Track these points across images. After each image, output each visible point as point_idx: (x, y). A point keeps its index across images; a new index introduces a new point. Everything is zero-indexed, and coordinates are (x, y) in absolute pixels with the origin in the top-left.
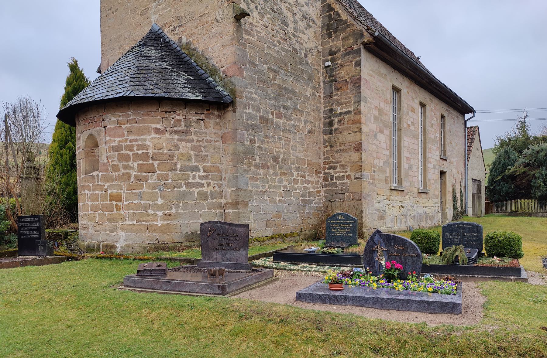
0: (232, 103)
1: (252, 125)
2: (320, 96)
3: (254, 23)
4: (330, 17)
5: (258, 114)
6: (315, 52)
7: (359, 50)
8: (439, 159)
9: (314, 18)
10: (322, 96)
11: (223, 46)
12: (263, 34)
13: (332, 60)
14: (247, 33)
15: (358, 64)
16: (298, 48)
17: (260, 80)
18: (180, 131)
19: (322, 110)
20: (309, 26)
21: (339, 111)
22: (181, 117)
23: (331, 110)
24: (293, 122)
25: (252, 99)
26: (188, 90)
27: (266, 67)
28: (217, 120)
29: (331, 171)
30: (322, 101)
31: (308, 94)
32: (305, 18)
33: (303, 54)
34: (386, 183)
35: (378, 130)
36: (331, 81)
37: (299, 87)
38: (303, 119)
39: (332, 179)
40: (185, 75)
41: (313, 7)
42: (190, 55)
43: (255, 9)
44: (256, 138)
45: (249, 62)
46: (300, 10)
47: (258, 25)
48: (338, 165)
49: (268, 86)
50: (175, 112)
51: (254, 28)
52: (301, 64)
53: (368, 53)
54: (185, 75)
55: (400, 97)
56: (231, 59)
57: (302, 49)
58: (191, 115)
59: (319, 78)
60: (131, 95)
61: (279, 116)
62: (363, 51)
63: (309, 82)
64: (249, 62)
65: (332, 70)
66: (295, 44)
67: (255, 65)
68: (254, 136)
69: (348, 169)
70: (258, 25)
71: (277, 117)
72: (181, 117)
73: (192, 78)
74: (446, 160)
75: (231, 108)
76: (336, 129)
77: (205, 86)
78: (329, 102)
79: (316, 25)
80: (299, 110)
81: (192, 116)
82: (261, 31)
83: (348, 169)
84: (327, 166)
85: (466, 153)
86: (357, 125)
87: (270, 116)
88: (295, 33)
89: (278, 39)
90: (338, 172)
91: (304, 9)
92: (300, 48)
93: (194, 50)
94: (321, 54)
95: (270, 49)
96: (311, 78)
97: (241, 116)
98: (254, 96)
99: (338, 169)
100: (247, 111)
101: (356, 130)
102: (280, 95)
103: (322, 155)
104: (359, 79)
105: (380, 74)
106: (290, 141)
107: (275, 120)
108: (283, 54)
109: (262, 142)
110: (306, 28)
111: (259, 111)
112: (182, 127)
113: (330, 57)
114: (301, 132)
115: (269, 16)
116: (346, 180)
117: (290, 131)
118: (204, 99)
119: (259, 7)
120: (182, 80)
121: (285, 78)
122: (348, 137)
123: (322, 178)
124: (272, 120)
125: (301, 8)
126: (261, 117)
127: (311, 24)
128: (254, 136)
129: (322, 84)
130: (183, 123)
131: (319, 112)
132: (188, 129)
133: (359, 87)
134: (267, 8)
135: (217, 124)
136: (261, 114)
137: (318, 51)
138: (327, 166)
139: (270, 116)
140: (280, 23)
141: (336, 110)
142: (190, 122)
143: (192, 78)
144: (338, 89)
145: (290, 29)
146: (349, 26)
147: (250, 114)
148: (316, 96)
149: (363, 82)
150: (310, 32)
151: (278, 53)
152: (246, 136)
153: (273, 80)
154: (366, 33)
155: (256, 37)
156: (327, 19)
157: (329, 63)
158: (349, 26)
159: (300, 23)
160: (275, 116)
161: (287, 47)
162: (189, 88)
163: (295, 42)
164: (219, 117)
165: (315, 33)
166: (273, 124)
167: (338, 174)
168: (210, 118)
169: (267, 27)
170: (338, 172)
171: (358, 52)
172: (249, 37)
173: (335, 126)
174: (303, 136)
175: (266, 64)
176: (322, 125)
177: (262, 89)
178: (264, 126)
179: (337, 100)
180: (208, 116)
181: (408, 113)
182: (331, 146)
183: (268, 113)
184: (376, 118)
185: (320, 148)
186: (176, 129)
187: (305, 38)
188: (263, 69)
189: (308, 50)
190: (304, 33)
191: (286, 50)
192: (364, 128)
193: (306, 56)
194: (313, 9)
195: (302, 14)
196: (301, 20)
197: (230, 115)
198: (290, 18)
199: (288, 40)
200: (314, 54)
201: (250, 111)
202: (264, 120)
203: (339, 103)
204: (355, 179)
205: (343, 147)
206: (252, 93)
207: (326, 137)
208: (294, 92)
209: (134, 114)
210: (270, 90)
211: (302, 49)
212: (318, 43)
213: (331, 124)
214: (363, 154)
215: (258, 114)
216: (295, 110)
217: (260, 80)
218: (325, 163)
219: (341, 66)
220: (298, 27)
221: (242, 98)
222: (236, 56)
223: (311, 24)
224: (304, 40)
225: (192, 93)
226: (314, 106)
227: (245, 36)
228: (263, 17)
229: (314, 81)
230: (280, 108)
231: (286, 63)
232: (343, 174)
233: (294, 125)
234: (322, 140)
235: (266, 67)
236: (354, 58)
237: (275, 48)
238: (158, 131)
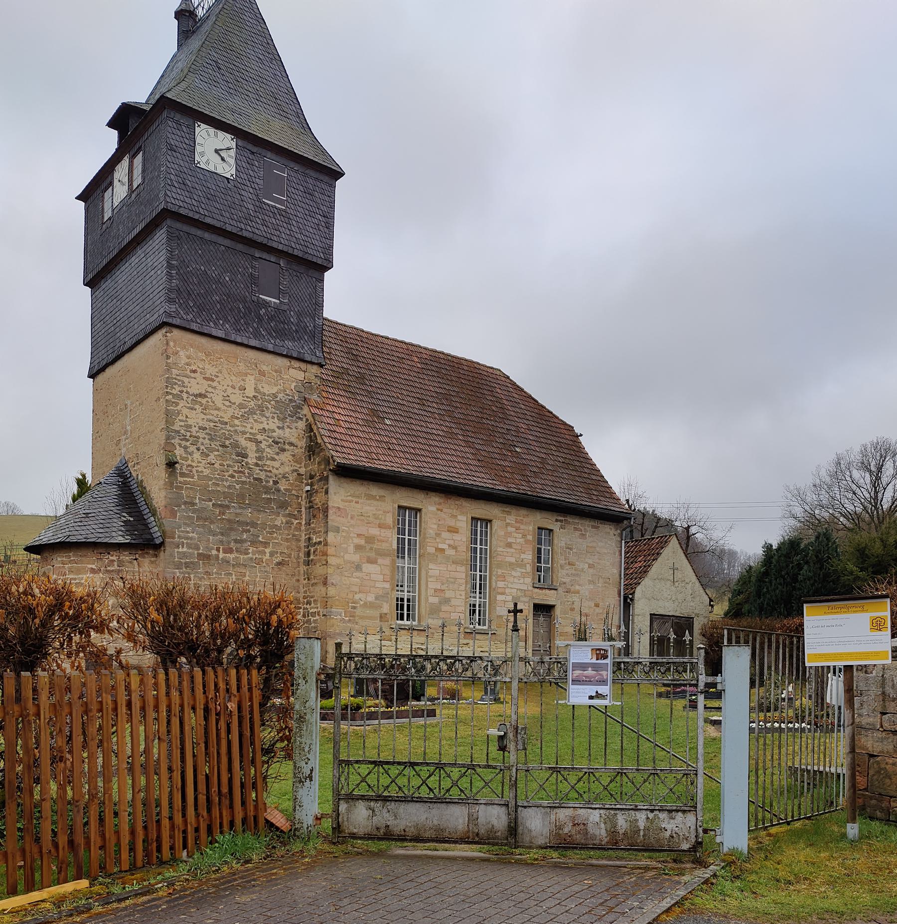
0: (162, 544)
1: (186, 563)
2: (300, 523)
3: (194, 464)
4: (310, 437)
5: (196, 552)
6: (292, 477)
7: (328, 476)
8: (532, 588)
9: (293, 440)
10: (304, 523)
11: (160, 489)
12: (207, 472)
13: (312, 485)
14: (183, 475)
15: (327, 492)
16: (263, 477)
17: (199, 518)
18: (113, 571)
19: (303, 538)
20: (283, 450)
21: (314, 541)
22: (114, 558)
23: (309, 539)
24: (250, 555)
25: (187, 538)
26: (120, 533)
27: (211, 503)
28: (152, 559)
29: (308, 606)
30: (303, 528)
31: (278, 523)
32: (277, 443)
33: (271, 482)
34: (381, 621)
35: (365, 561)
36: (310, 507)
37: (261, 518)
38: (267, 551)
39: (308, 616)
40: (125, 517)
41: (291, 428)
42: (142, 493)
43: (195, 451)
44: (192, 576)
45: (185, 503)
46: (268, 437)
47: (199, 465)
48: (312, 600)
49: (212, 522)
50: (109, 553)
51: (194, 470)
52: (266, 493)
53: (343, 480)
54: (125, 517)
55: (421, 517)
56: (164, 503)
57: (271, 477)
58: (124, 555)
59: (300, 504)
60: (67, 540)
61: (230, 551)
62: (331, 478)
63: (279, 510)
64: (185, 503)
65: (311, 495)
66: (257, 474)
67: (194, 504)
68: (189, 574)
69: (319, 605)
70: (199, 465)
71: (224, 552)
72: (114, 558)
73: (132, 519)
74: (556, 589)
75: (162, 549)
76: (312, 560)
77: (143, 527)
78: (308, 530)
79: (297, 446)
80: (262, 542)
81: (126, 557)
82: (204, 470)
83: (319, 605)
84: (305, 600)
85: (622, 576)
86: (325, 557)
87: (214, 552)
88: (259, 462)
89: (230, 473)
90: (313, 608)
91: (274, 434)
92: (267, 476)
93: (145, 488)
94: (304, 477)
95: (218, 485)
96: (283, 505)
97: (172, 555)
98: (191, 535)
99: (312, 605)
100: (180, 550)
101: (324, 563)
102: (231, 529)
103: (301, 587)
104: (327, 508)
105: (370, 497)
106: (245, 576)
107: (221, 555)
108: (237, 487)
109: (200, 579)
110: (278, 454)
111: (198, 549)
112: (115, 567)
113: (310, 481)
114: (264, 564)
115: (216, 453)
116: (317, 617)
117: (245, 566)
118: (133, 541)
119: (202, 447)
120: (120, 523)
121: (238, 511)
122: (318, 570)
123: (302, 613)
124: (217, 556)
125: (270, 434)
126: (199, 554)
127: (287, 447)
128: (189, 574)
129: (303, 509)
130: (116, 563)
131: (298, 540)
132: (121, 568)
133: (327, 516)
134: (213, 446)
135: (152, 562)
136: (201, 551)
137: (299, 474)
138: (305, 600)
139: (214, 552)
140: (234, 457)
141: (312, 539)
142: (123, 562)
143: (132, 519)
144: (314, 517)
145: (251, 460)
146: (323, 450)
147: (184, 553)
148: (293, 523)
149: (331, 512)
150: (286, 457)
151: (229, 487)
152: (178, 574)
153: (219, 516)
154: (331, 461)
155: (196, 477)
156: (308, 439)
157: (308, 488)
158: (323, 450)
159: (268, 450)
160: (221, 551)
161: (244, 479)
162: (122, 531)
163: (258, 471)
164: (156, 556)
165: (294, 456)
166: (218, 560)
167: (312, 610)
168: (144, 557)
169: (213, 464)
170: (313, 608)
171: (326, 479)
172: (185, 479)
173: (312, 557)
174: (268, 569)
175: (211, 500)
176: (302, 555)
177: (203, 526)
178: (203, 563)
179: (313, 528)
180: (142, 556)
181: (438, 535)
182: (308, 580)
183: (212, 549)
184: (358, 548)
185: (298, 581)
186: (109, 568)
187: (276, 464)
188: (205, 506)
189: (280, 476)
190: (273, 459)
191: (243, 483)
192: (332, 560)
193: (276, 483)
194: (291, 431)
195: (271, 440)
196: (269, 446)
197: (162, 553)
198: (251, 448)
199: (246, 471)
200: (291, 478)
201: (185, 549)
202: (205, 557)
203: (315, 533)
204: (324, 615)
205: (316, 581)
206: (188, 532)
207: (305, 568)
208: (254, 525)
209: (74, 555)
210: (215, 526)
211: (271, 477)
212: (299, 466)
213: (308, 554)
214: (329, 589)
215: (196, 552)
216: (254, 543)
217: (199, 518)
218: (304, 597)
219: (317, 492)
220: (264, 455)
221: (174, 538)
222: (168, 500)
223: (287, 447)
224: (273, 467)
225: (123, 536)
226: (289, 535)
227: (181, 479)
228: (208, 455)
229: (289, 508)
230: (229, 543)
231: (241, 496)
232: (316, 610)
233: (252, 559)
234: (302, 572)
235: (211, 503)
236: (324, 485)
237: (225, 483)
238: (93, 571)
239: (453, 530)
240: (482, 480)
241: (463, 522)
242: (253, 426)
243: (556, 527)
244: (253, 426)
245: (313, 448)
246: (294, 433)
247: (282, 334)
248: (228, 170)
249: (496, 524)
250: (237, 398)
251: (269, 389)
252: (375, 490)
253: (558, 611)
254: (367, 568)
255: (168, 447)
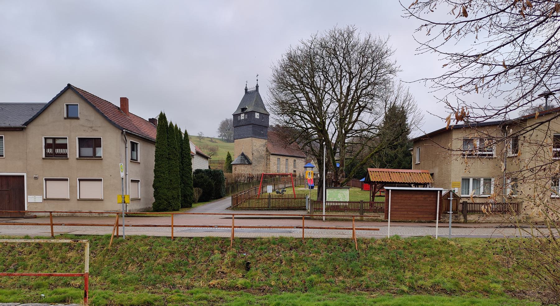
81: (247, 165)
96: (264, 158)
122: (268, 167)
239: (284, 161)
240: (287, 154)
241: (285, 160)
242: (260, 148)
243: (296, 160)
244: (260, 148)
245: (267, 151)
246: (265, 149)
247: (263, 136)
248: (258, 118)
249: (289, 160)
250: (259, 145)
251: (262, 143)
252: (275, 156)
253: (297, 172)
254: (274, 166)
255: (252, 152)
